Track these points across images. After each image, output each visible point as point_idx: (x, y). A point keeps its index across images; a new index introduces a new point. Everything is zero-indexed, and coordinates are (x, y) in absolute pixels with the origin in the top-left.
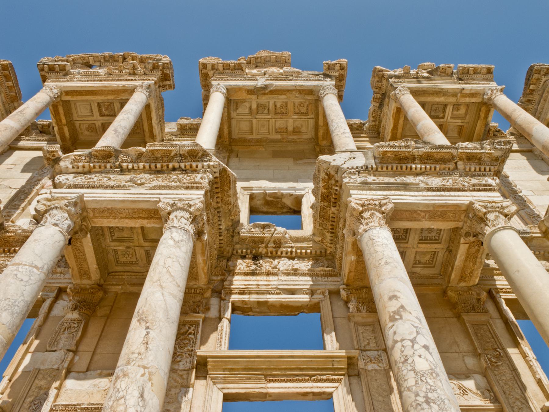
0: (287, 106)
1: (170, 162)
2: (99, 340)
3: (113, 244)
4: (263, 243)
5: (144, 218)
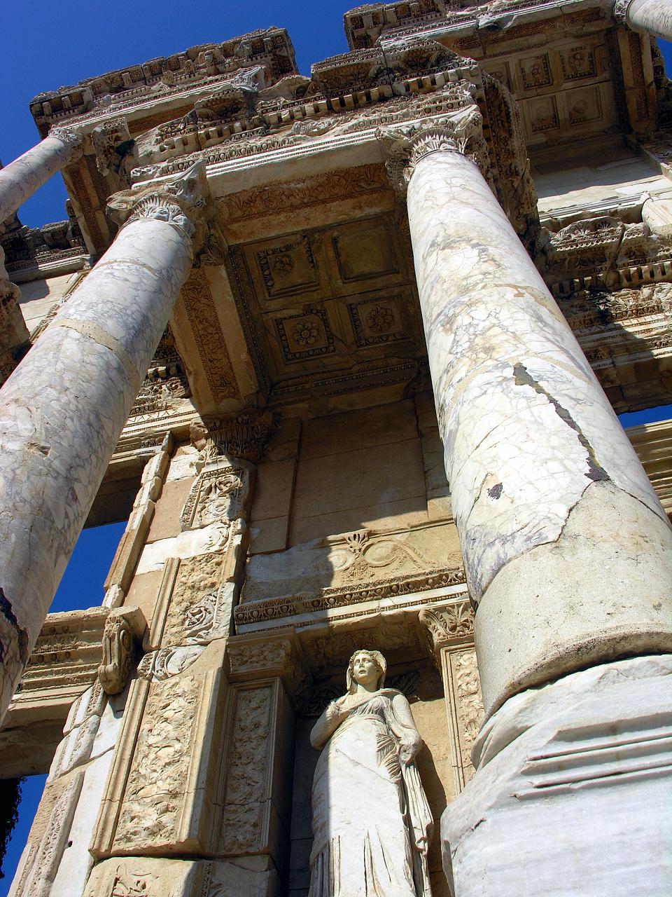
0: (546, 65)
1: (372, 87)
2: (293, 497)
3: (273, 305)
4: (603, 260)
5: (345, 197)
